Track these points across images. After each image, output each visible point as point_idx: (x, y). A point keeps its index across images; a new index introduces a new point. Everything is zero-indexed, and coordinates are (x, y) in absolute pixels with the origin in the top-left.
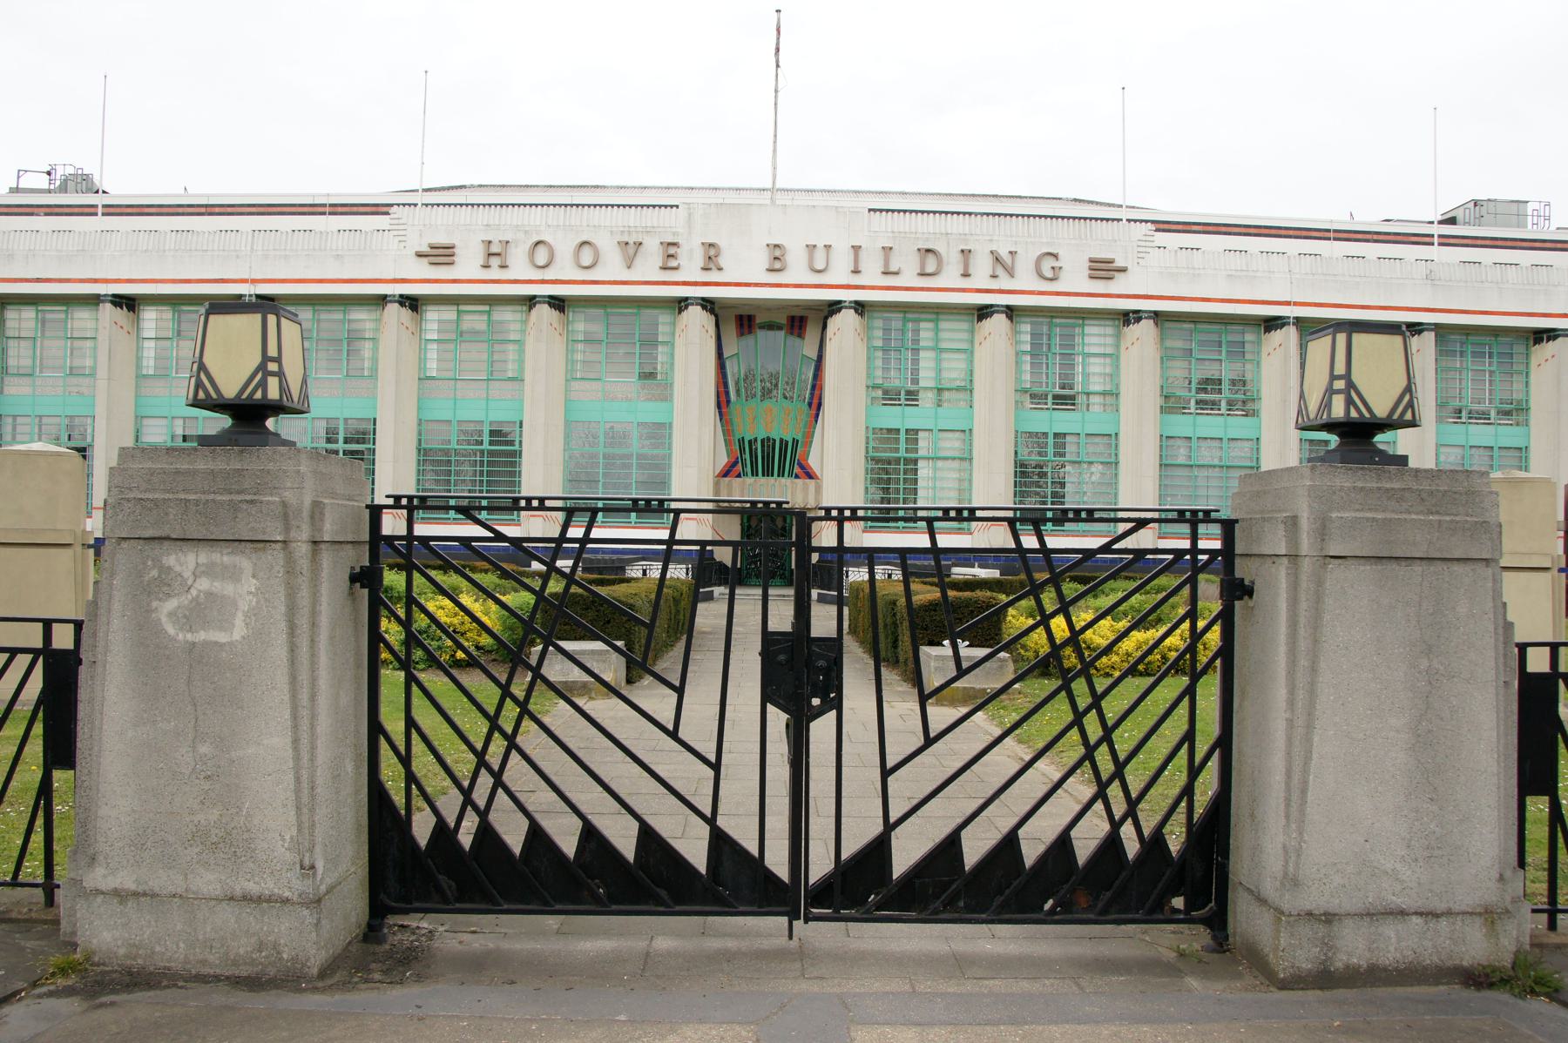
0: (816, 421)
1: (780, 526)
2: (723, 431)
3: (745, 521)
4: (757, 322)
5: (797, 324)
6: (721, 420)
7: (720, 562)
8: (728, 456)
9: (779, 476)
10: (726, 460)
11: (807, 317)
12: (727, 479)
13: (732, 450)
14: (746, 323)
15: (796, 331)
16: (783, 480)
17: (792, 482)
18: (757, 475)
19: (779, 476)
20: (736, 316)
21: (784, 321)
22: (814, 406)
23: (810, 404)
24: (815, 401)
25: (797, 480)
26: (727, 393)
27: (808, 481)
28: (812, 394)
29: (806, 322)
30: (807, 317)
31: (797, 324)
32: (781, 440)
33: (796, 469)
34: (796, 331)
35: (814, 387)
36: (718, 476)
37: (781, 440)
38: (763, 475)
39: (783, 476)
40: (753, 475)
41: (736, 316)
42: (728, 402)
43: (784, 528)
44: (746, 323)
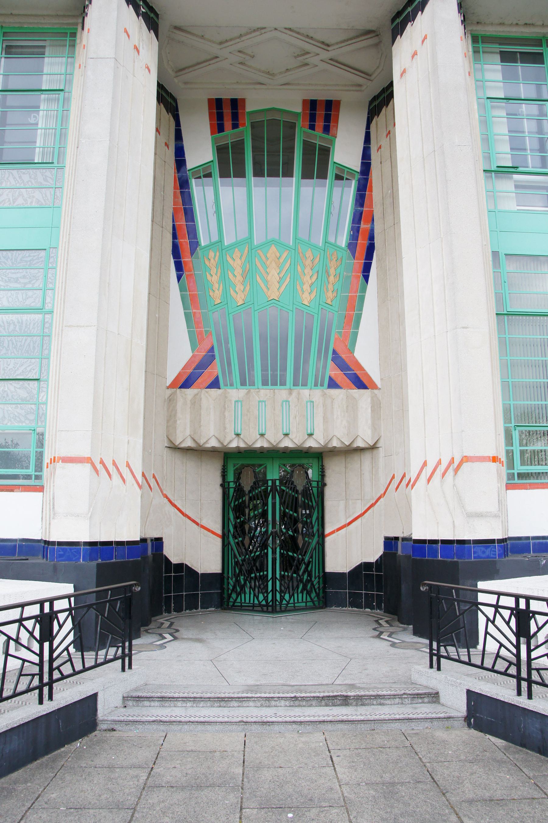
0: (366, 278)
1: (300, 488)
2: (183, 298)
3: (231, 477)
4: (249, 108)
5: (320, 113)
6: (179, 278)
7: (180, 567)
8: (193, 350)
9: (296, 384)
10: (191, 354)
11: (338, 103)
12: (190, 392)
13: (200, 333)
14: (227, 111)
15: (320, 123)
16: (305, 392)
17: (324, 395)
18: (252, 384)
19: (296, 384)
20: (210, 101)
21: (298, 109)
22: (361, 250)
23: (352, 246)
24: (363, 242)
25: (334, 392)
26: (193, 233)
27: (356, 392)
28: (355, 231)
29: (338, 110)
30: (338, 103)
31: (320, 113)
32: (299, 312)
33: (331, 370)
34: (320, 123)
35: (357, 218)
36: (172, 386)
37: (299, 312)
38: (265, 383)
39: (305, 384)
40: (243, 383)
41: (210, 101)
42: (194, 245)
43: (306, 493)
44: (227, 111)
